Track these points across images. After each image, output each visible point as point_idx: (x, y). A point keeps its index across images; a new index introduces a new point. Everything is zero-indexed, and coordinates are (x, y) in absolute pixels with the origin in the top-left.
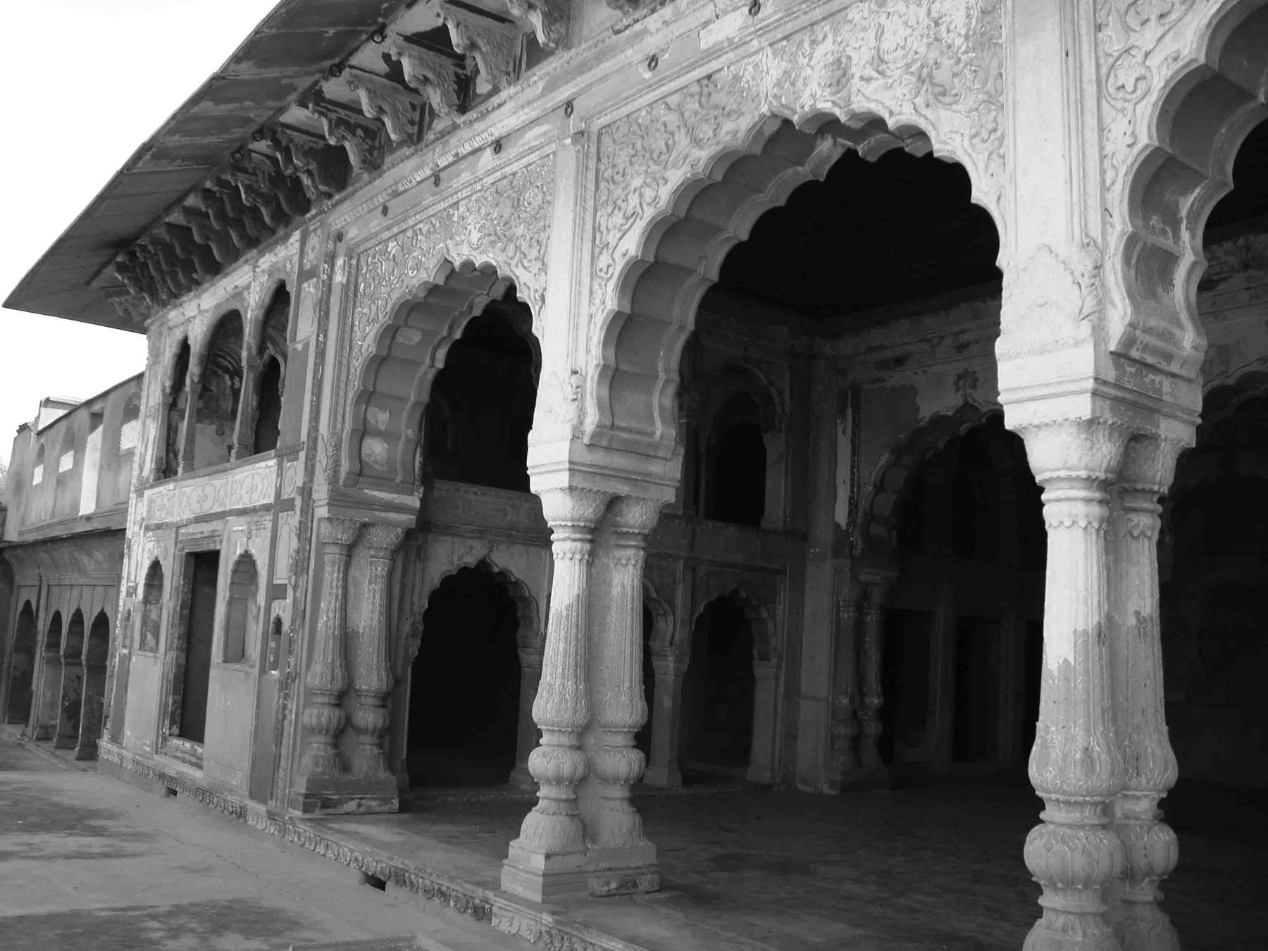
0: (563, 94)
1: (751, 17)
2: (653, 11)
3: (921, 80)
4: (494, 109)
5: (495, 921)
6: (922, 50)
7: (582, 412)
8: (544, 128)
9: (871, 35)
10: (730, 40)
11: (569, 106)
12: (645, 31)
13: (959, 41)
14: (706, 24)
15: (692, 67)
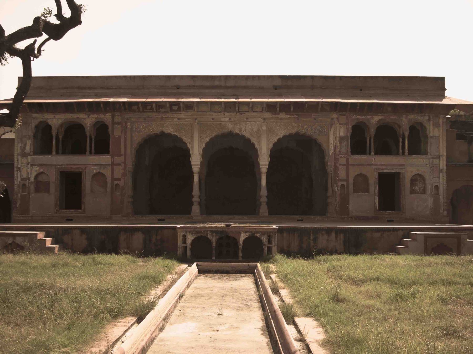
0: (195, 117)
1: (229, 120)
2: (214, 113)
3: (251, 134)
4: (178, 113)
5: (193, 219)
6: (251, 131)
7: (201, 159)
8: (190, 120)
9: (244, 127)
10: (226, 121)
11: (196, 118)
12: (212, 115)
13: (255, 132)
14: (222, 118)
15: (219, 121)
